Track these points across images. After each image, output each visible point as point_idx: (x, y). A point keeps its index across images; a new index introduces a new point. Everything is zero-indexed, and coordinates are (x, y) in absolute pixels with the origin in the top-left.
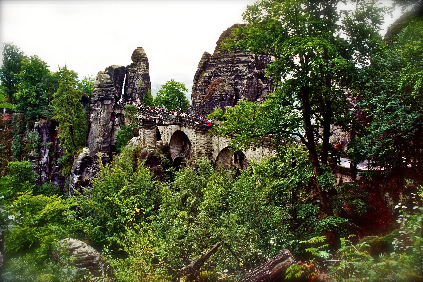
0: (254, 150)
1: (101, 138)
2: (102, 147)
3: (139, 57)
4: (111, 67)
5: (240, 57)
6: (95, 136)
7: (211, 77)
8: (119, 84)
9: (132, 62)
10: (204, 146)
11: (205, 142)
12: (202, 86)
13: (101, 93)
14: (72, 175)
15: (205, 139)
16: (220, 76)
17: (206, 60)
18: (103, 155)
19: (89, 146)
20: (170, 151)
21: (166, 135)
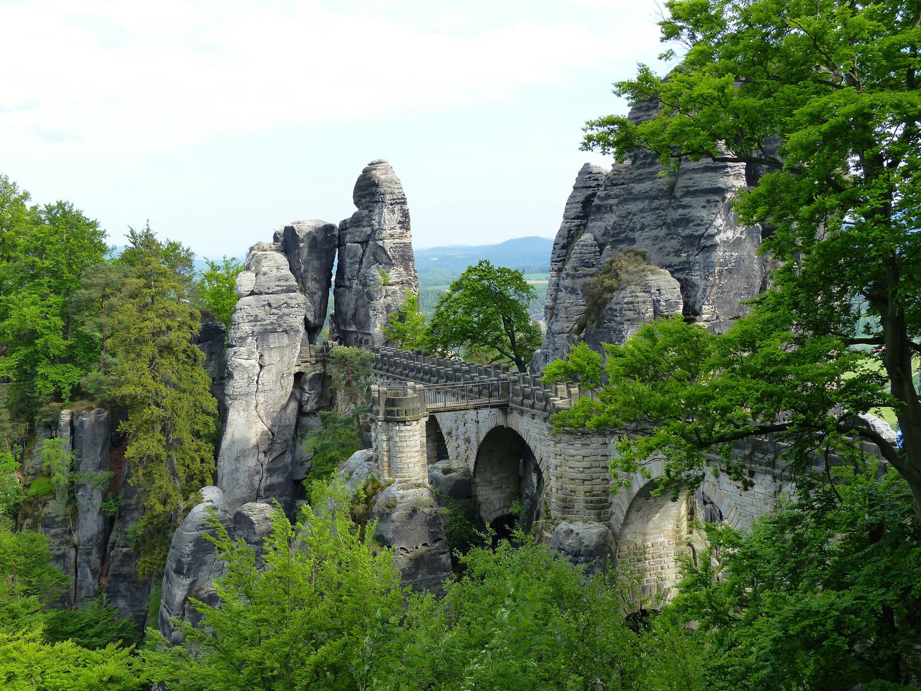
0: (746, 489)
1: (262, 456)
2: (263, 484)
3: (368, 190)
4: (292, 228)
5: (697, 176)
6: (243, 451)
7: (602, 246)
8: (318, 281)
9: (355, 209)
10: (580, 476)
11: (586, 464)
12: (573, 277)
13: (261, 313)
14: (168, 576)
15: (584, 452)
16: (632, 241)
17: (590, 192)
18: (262, 510)
19: (224, 484)
20: (476, 496)
21: (461, 442)
